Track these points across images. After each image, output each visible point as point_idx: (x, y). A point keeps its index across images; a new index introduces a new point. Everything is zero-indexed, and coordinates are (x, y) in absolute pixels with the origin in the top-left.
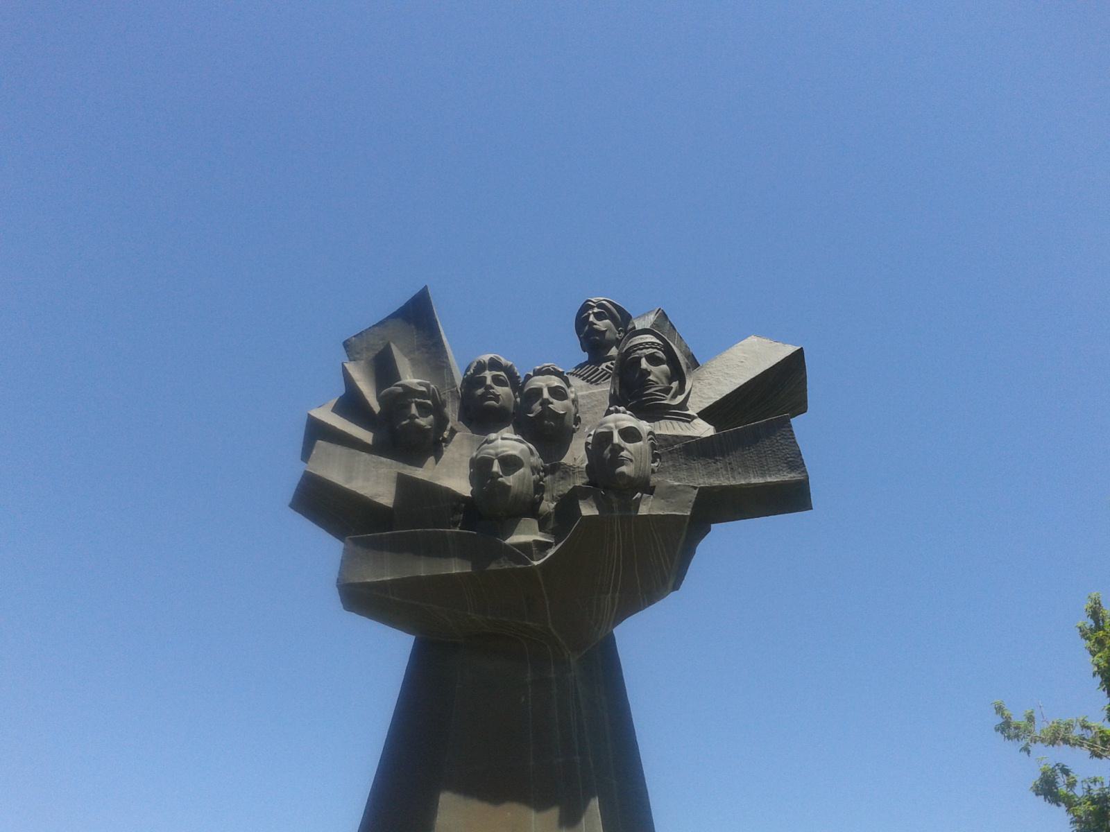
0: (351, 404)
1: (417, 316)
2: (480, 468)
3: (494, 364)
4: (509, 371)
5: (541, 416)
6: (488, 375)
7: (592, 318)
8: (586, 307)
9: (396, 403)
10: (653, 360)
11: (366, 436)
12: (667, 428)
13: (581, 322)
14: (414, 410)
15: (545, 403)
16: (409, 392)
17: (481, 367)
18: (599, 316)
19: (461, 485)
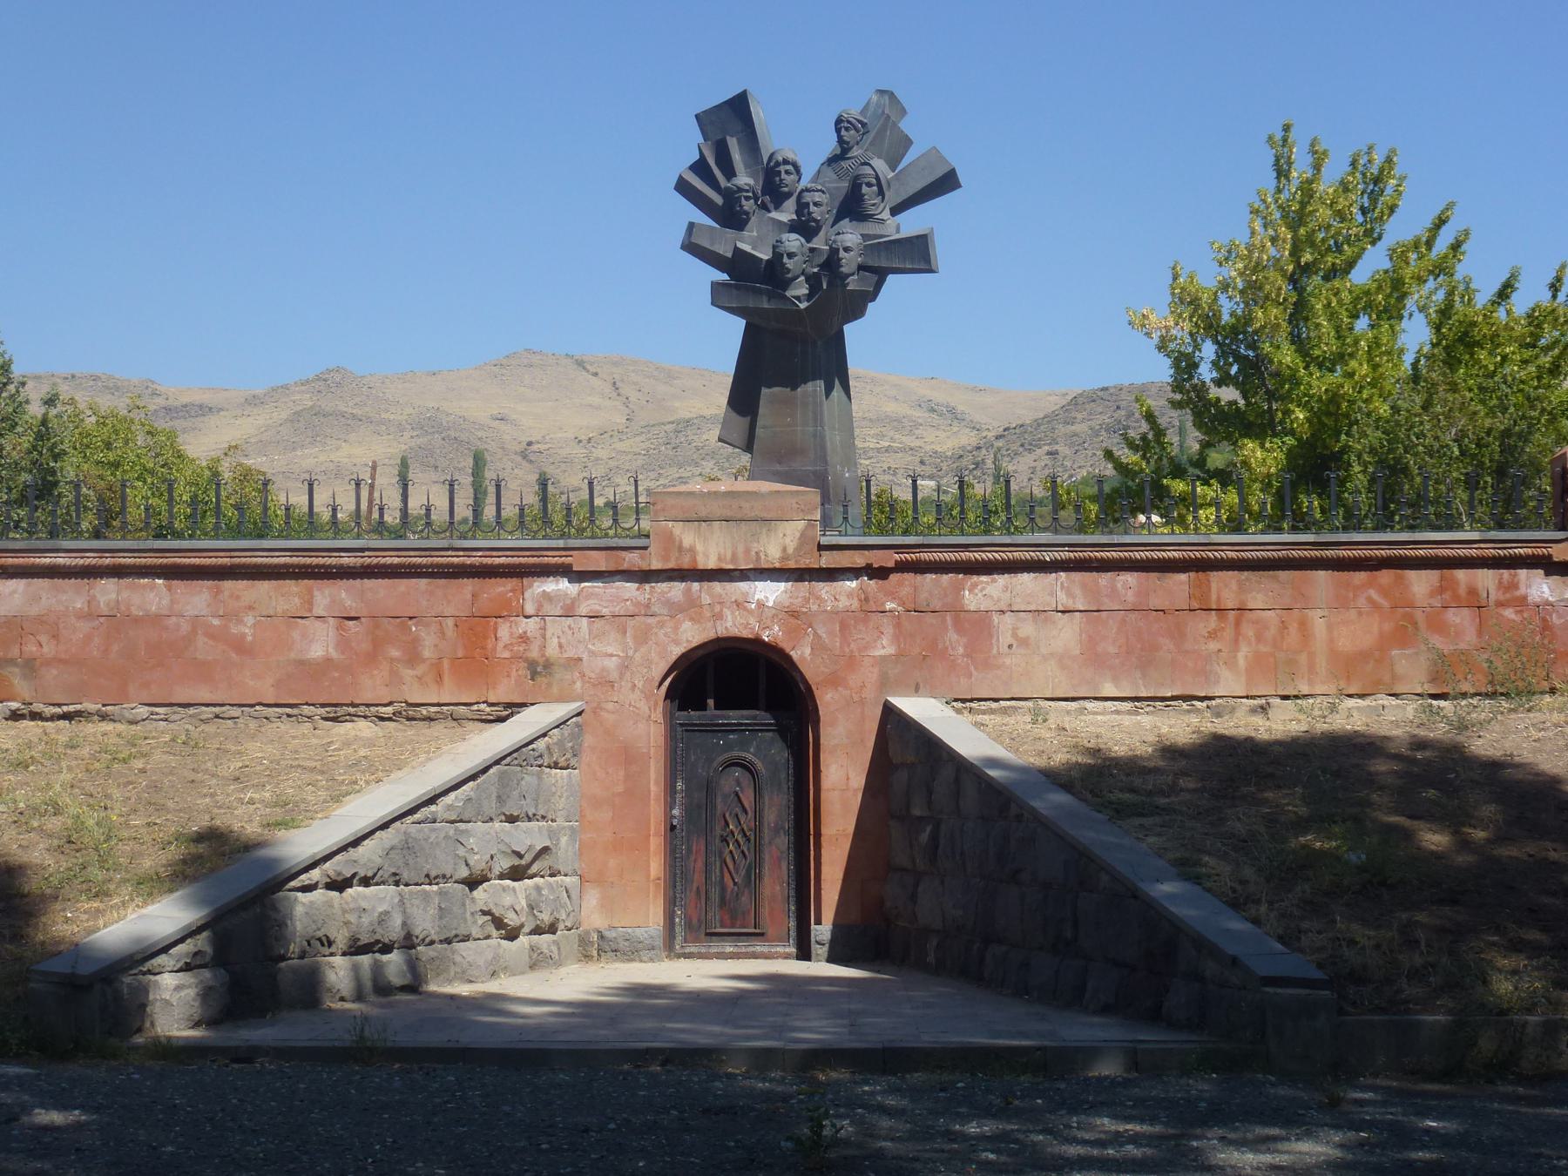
0: (700, 167)
1: (739, 107)
2: (777, 256)
3: (786, 162)
4: (795, 165)
5: (808, 221)
6: (782, 168)
7: (843, 132)
8: (839, 121)
9: (731, 196)
10: (869, 185)
11: (718, 200)
12: (870, 228)
13: (838, 131)
14: (744, 202)
15: (810, 213)
16: (740, 190)
17: (778, 164)
18: (847, 129)
19: (764, 255)
